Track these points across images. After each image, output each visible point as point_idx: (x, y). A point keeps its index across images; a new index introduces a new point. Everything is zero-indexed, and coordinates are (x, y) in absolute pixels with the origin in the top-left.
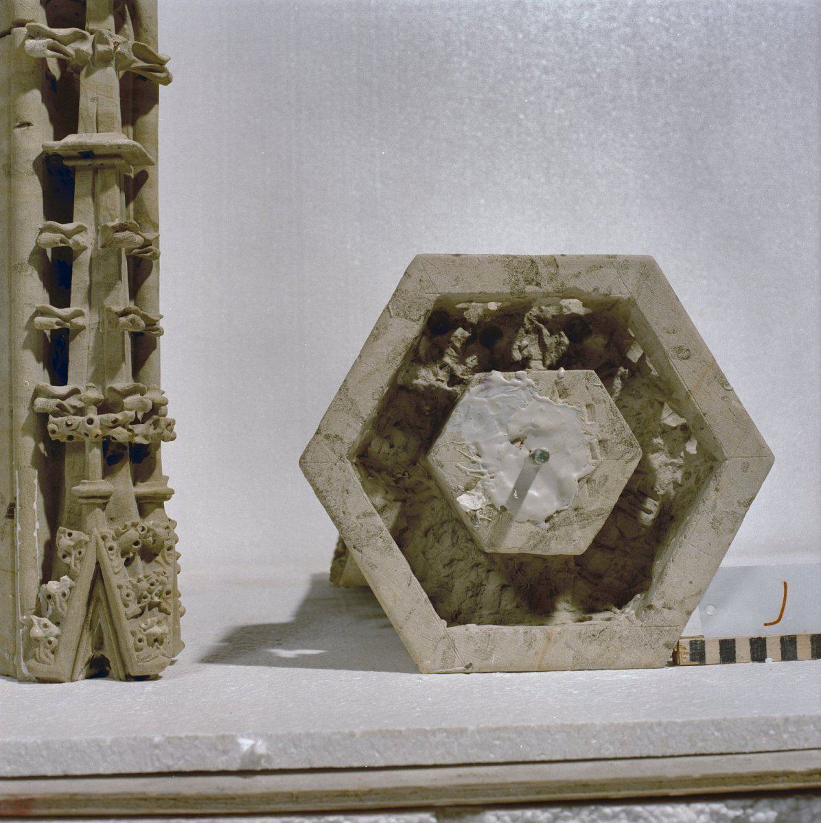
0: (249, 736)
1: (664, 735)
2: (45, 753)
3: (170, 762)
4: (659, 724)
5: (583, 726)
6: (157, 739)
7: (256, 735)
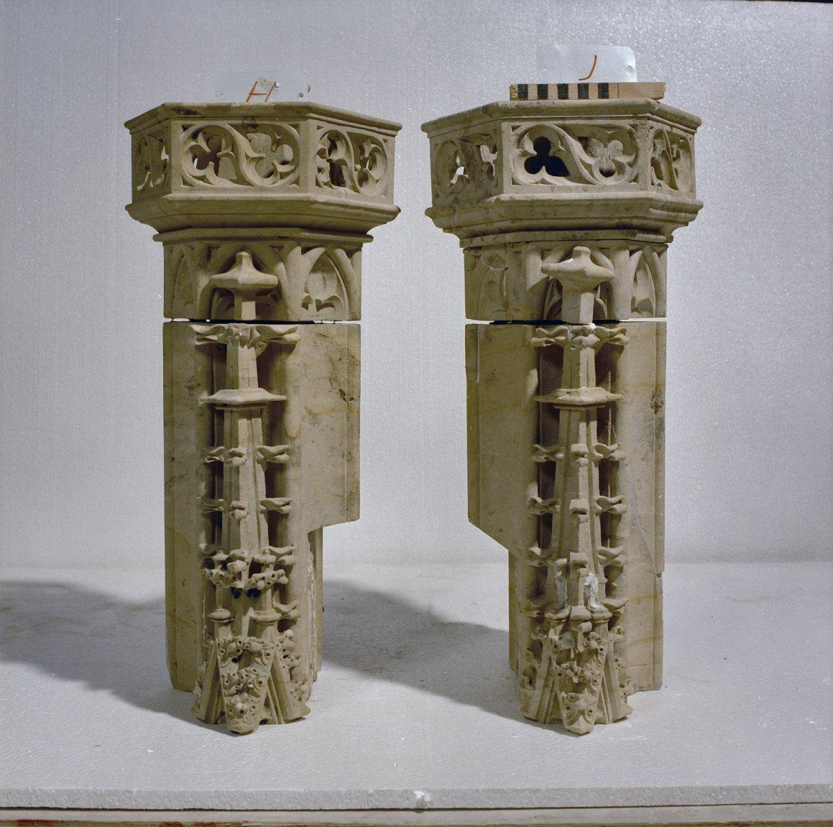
0: (420, 790)
1: (651, 795)
2: (309, 797)
3: (378, 804)
4: (649, 789)
5: (605, 788)
6: (370, 792)
7: (424, 789)
